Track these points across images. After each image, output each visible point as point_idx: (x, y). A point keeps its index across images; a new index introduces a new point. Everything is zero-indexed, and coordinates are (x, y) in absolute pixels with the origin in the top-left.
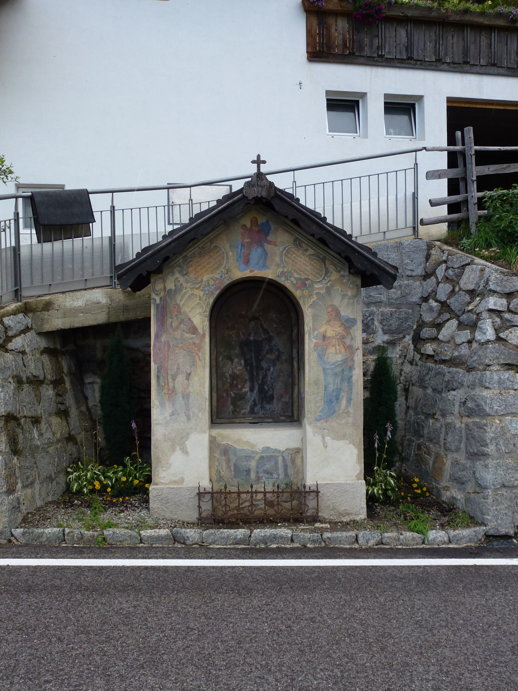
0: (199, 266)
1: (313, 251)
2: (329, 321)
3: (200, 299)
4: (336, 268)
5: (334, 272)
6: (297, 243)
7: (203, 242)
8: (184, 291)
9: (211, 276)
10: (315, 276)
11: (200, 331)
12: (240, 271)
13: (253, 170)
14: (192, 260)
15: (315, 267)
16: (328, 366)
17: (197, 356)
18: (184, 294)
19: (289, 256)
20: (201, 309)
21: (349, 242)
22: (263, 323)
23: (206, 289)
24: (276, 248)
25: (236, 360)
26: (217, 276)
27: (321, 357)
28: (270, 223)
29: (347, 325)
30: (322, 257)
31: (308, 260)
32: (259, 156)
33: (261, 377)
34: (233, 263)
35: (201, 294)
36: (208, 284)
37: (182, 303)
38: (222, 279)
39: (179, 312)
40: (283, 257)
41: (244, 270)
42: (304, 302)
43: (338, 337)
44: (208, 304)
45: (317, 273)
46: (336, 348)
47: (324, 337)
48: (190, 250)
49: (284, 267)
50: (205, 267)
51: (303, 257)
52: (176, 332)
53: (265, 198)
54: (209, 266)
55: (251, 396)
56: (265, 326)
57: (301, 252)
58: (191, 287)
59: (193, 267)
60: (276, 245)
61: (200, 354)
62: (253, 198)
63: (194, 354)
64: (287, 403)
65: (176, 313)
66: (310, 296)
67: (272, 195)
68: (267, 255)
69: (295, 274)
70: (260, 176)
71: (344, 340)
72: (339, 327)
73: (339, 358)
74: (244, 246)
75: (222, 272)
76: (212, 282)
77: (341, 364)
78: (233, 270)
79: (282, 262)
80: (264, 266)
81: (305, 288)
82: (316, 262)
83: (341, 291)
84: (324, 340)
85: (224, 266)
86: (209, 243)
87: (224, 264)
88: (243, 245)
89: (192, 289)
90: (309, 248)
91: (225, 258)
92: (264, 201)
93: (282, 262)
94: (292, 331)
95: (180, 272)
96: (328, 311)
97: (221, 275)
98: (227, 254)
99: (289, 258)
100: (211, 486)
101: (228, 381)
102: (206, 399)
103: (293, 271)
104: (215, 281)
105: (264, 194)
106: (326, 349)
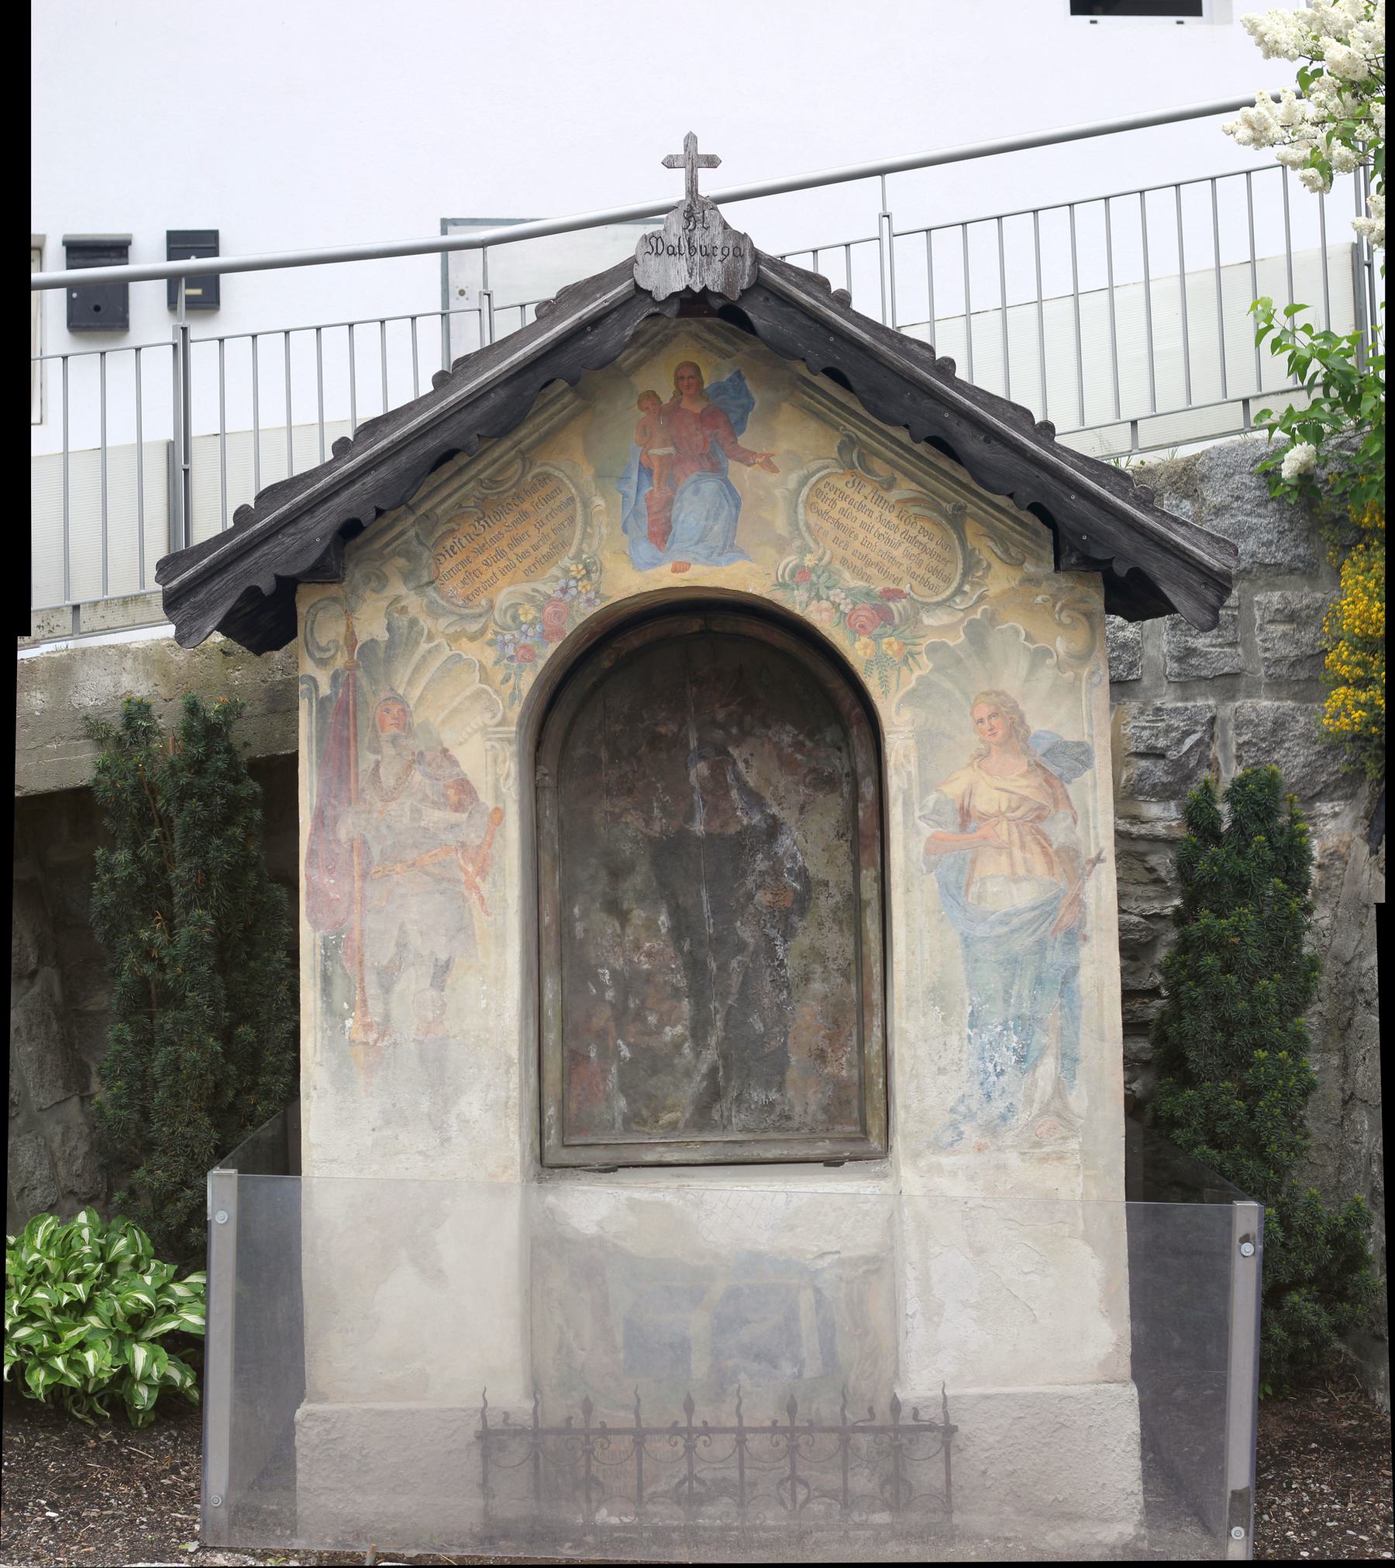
0: (482, 549)
1: (914, 486)
2: (982, 756)
3: (485, 678)
4: (1006, 551)
5: (997, 565)
6: (854, 458)
7: (495, 461)
8: (424, 646)
9: (526, 588)
10: (925, 582)
11: (486, 798)
12: (638, 567)
13: (672, 189)
14: (453, 531)
15: (925, 549)
16: (981, 930)
17: (474, 897)
18: (424, 659)
19: (824, 507)
20: (489, 715)
21: (1044, 453)
22: (741, 766)
23: (508, 637)
24: (772, 478)
25: (638, 915)
26: (549, 589)
27: (955, 891)
28: (749, 384)
29: (1051, 768)
30: (948, 507)
31: (895, 521)
32: (691, 140)
33: (735, 981)
34: (614, 539)
35: (489, 655)
36: (515, 618)
37: (417, 692)
38: (567, 598)
39: (404, 722)
40: (801, 510)
41: (654, 565)
42: (884, 681)
43: (1019, 813)
44: (513, 698)
45: (934, 571)
46: (1010, 855)
47: (965, 815)
48: (445, 492)
49: (804, 550)
50: (501, 554)
51: (877, 510)
52: (393, 805)
53: (720, 295)
54: (519, 550)
55: (698, 1055)
56: (751, 779)
57: (867, 490)
58: (451, 630)
59: (460, 557)
60: (769, 465)
61: (485, 888)
62: (674, 295)
63: (462, 888)
64: (840, 1085)
65: (394, 730)
66: (908, 657)
67: (745, 283)
68: (738, 507)
69: (847, 575)
70: (696, 210)
71: (1044, 826)
72: (1023, 776)
73: (1024, 896)
74: (650, 473)
75: (566, 571)
76: (528, 613)
77: (1031, 922)
78: (608, 565)
79: (796, 530)
80: (729, 548)
81: (889, 629)
82: (927, 526)
83: (1028, 637)
84: (963, 826)
85: (573, 550)
86: (518, 465)
87: (576, 542)
88: (645, 470)
89: (454, 638)
90: (898, 475)
91: (579, 519)
92: (717, 304)
93: (796, 530)
94: (856, 797)
95: (407, 576)
96: (977, 716)
97: (562, 583)
98: (586, 505)
99: (821, 514)
100: (529, 1405)
101: (610, 995)
102: (509, 1060)
103: (837, 565)
104: (541, 609)
105: (712, 279)
106: (974, 862)
